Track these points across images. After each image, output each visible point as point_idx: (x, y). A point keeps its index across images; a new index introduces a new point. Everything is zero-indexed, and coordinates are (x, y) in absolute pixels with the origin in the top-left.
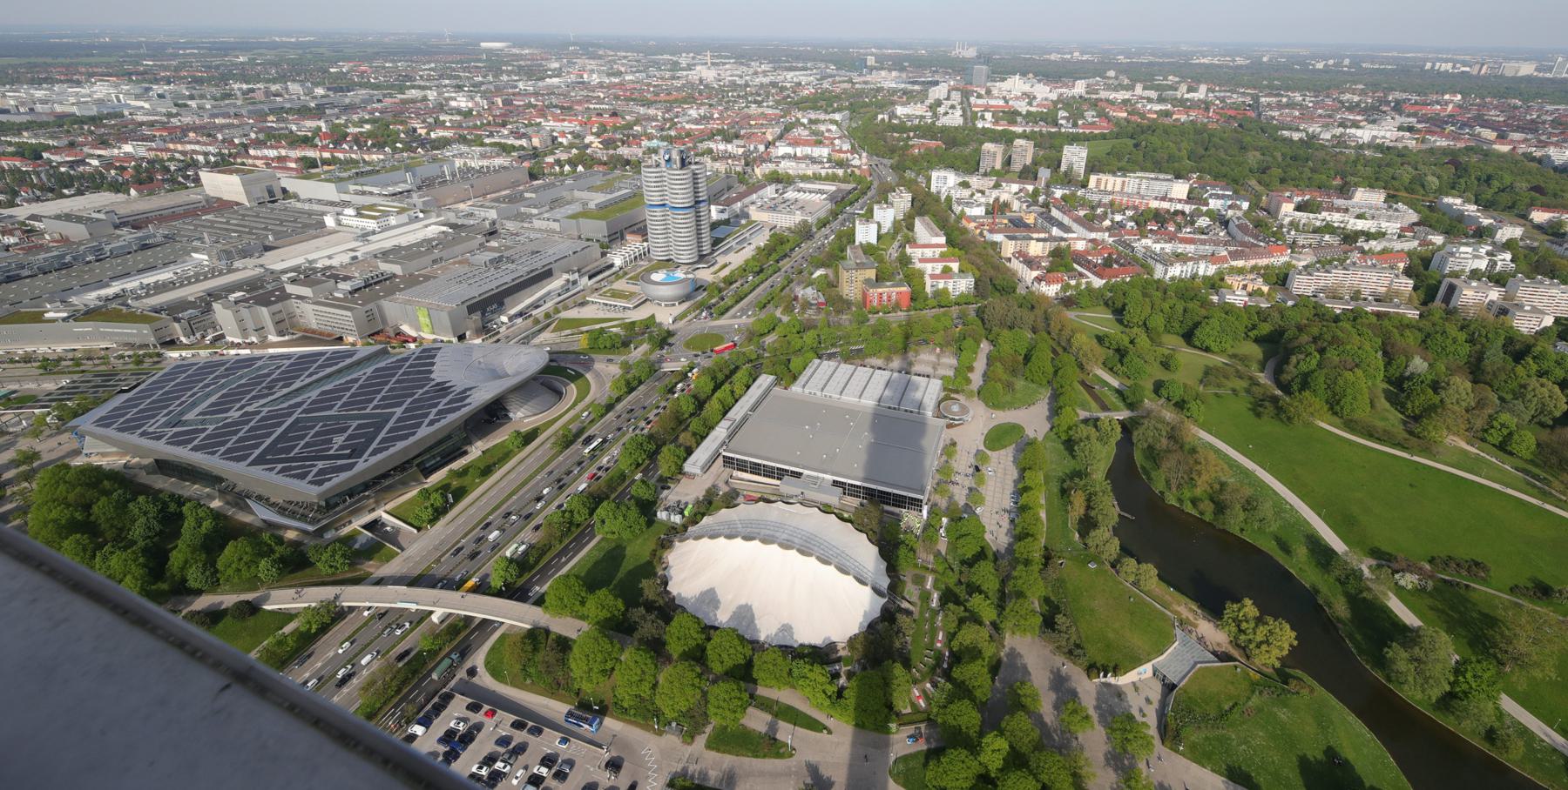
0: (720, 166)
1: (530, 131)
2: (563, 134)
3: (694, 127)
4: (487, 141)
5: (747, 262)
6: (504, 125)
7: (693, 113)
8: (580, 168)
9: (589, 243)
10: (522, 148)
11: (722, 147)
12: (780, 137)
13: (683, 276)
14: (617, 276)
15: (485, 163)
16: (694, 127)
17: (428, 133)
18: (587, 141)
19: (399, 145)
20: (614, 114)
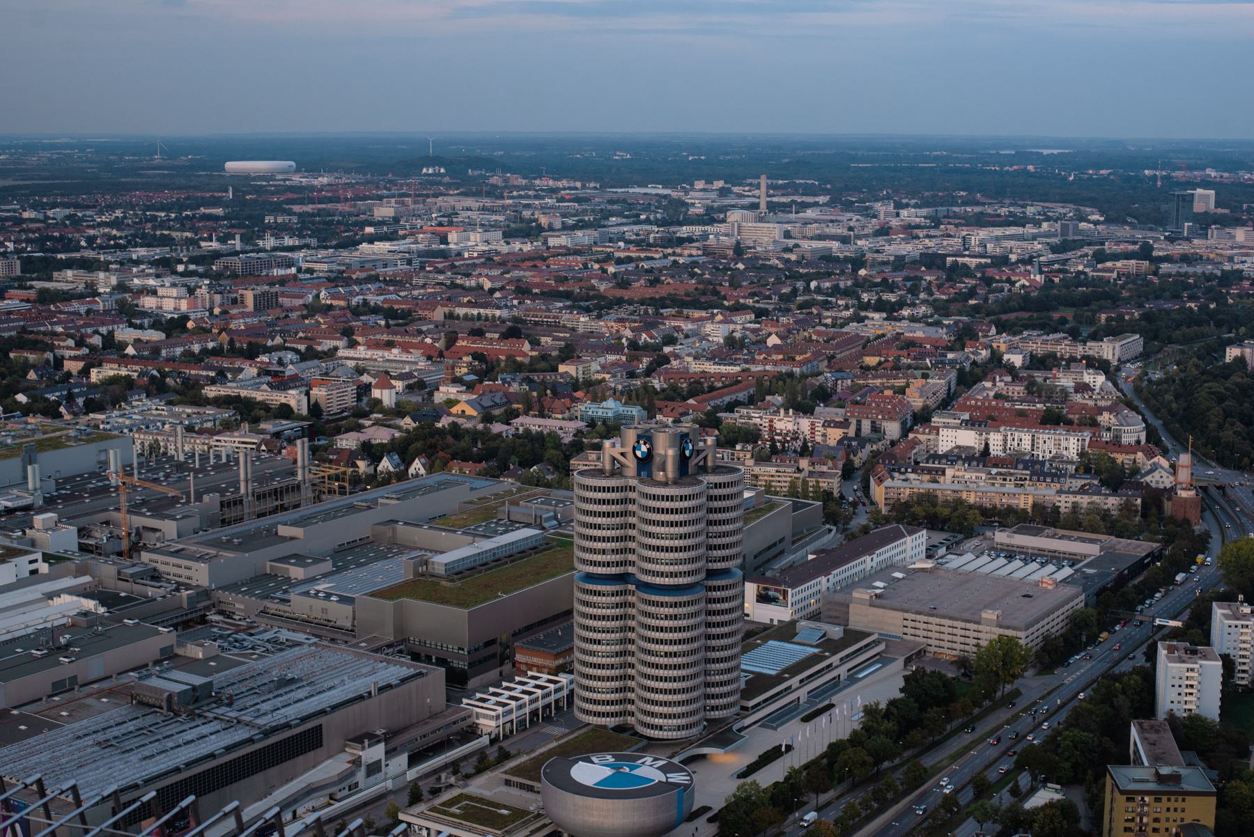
0: (777, 474)
1: (312, 370)
2: (385, 378)
3: (711, 368)
4: (211, 392)
5: (835, 749)
6: (251, 353)
7: (716, 332)
8: (417, 466)
9: (422, 667)
10: (285, 412)
11: (785, 423)
12: (946, 404)
13: (659, 777)
14: (483, 764)
15: (198, 444)
16: (711, 368)
17: (85, 372)
18: (439, 397)
19: (21, 398)
20: (514, 331)
